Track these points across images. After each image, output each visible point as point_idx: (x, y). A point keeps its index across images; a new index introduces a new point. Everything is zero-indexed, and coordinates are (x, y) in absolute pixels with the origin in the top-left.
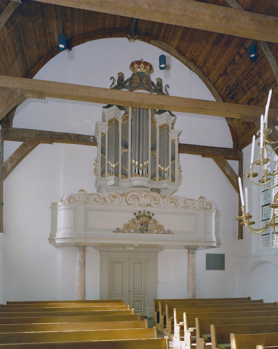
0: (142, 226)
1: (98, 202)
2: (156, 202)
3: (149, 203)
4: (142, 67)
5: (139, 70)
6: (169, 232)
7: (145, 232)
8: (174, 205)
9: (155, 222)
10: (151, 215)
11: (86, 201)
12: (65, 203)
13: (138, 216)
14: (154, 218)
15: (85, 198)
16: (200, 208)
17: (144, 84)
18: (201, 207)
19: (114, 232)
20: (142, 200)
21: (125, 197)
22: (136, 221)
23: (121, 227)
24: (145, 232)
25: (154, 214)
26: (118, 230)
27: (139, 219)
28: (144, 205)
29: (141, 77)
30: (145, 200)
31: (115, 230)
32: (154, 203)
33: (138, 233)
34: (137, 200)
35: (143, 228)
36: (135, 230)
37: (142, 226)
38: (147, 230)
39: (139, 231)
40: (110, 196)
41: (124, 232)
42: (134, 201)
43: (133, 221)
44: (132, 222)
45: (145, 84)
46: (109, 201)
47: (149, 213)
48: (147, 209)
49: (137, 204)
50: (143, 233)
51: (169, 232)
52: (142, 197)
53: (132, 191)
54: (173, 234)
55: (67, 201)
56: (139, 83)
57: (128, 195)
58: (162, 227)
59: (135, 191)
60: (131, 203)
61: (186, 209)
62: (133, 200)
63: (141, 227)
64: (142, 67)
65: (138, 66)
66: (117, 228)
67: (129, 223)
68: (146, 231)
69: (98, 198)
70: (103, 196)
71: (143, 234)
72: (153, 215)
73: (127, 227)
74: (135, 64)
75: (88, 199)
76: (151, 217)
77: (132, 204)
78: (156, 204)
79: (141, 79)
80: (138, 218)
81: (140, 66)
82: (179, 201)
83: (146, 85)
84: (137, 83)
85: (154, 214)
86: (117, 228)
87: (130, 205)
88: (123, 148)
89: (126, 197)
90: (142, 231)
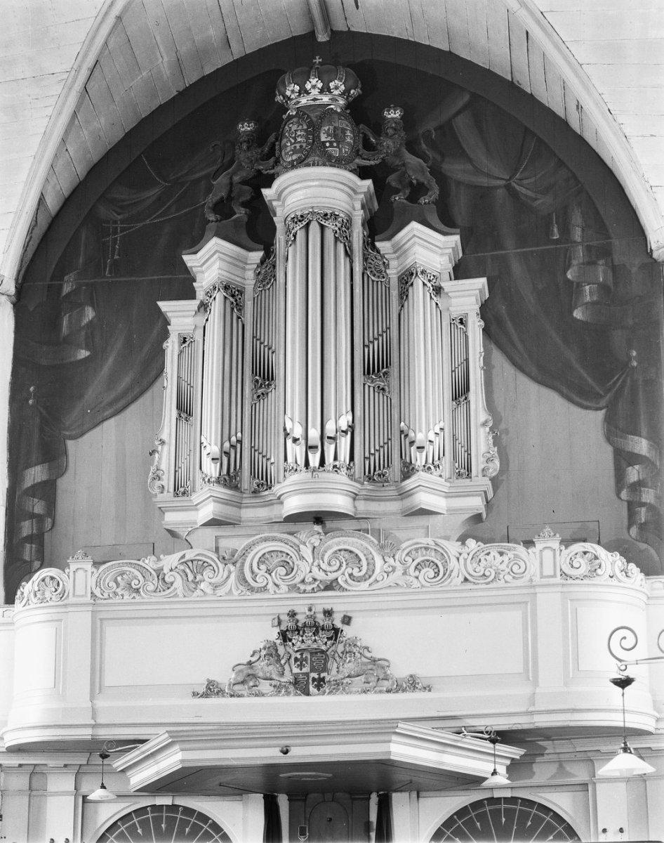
0: (301, 666)
1: (137, 591)
2: (356, 572)
3: (332, 576)
4: (336, 88)
5: (304, 101)
6: (413, 684)
7: (312, 689)
8: (432, 574)
9: (352, 648)
10: (338, 624)
11: (97, 592)
12: (29, 604)
13: (287, 630)
14: (348, 632)
15: (92, 582)
16: (542, 577)
17: (327, 147)
18: (548, 570)
19: (195, 694)
20: (303, 569)
21: (238, 565)
22: (281, 650)
23: (225, 677)
24: (312, 689)
25: (350, 618)
26: (212, 690)
27: (290, 640)
28: (309, 588)
29: (311, 124)
30: (315, 569)
31: (202, 689)
32: (351, 575)
33: (288, 693)
34: (282, 571)
35: (307, 674)
36: (273, 683)
37: (301, 666)
38: (320, 683)
39: (291, 688)
40: (182, 567)
41: (231, 696)
42: (273, 574)
43: (272, 652)
44: (264, 653)
45: (328, 144)
46: (179, 583)
47: (328, 613)
48: (325, 600)
49: (284, 588)
50: (308, 694)
51: (413, 684)
52: (302, 558)
53: (266, 540)
54: (428, 688)
55: (36, 596)
56: (304, 145)
57: (252, 554)
58: (383, 668)
59: (274, 539)
60: (261, 581)
61: (480, 586)
62: (269, 572)
63: (296, 670)
64: (336, 88)
65: (297, 88)
66: (208, 680)
67: (253, 659)
68: (318, 687)
69: (140, 577)
70: (155, 567)
71: (304, 699)
72: (347, 620)
73: (248, 678)
74: (290, 83)
75: (105, 581)
76: (337, 631)
77: (264, 589)
78: (359, 580)
79: (313, 129)
80: (284, 636)
81: (308, 86)
82: (454, 560)
83: (331, 146)
84: (298, 146)
85: (350, 618)
86: (208, 680)
87: (252, 589)
88: (257, 381)
89: (243, 564)
90: (300, 686)
